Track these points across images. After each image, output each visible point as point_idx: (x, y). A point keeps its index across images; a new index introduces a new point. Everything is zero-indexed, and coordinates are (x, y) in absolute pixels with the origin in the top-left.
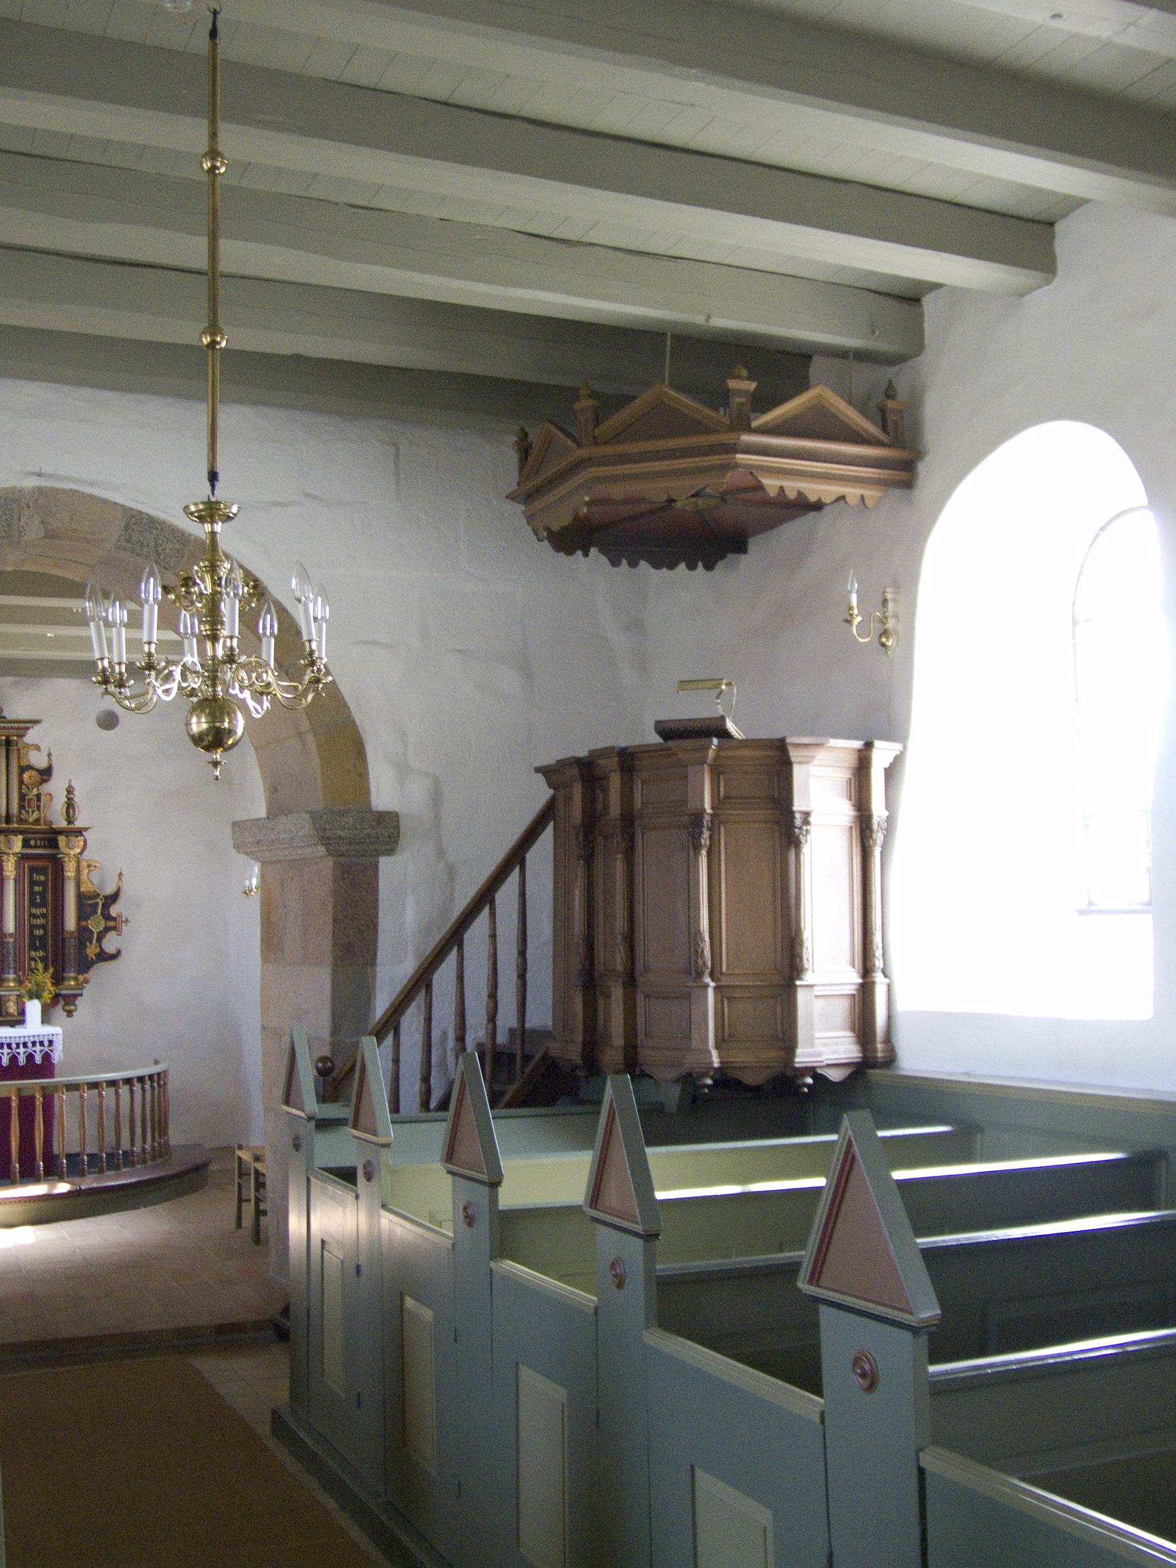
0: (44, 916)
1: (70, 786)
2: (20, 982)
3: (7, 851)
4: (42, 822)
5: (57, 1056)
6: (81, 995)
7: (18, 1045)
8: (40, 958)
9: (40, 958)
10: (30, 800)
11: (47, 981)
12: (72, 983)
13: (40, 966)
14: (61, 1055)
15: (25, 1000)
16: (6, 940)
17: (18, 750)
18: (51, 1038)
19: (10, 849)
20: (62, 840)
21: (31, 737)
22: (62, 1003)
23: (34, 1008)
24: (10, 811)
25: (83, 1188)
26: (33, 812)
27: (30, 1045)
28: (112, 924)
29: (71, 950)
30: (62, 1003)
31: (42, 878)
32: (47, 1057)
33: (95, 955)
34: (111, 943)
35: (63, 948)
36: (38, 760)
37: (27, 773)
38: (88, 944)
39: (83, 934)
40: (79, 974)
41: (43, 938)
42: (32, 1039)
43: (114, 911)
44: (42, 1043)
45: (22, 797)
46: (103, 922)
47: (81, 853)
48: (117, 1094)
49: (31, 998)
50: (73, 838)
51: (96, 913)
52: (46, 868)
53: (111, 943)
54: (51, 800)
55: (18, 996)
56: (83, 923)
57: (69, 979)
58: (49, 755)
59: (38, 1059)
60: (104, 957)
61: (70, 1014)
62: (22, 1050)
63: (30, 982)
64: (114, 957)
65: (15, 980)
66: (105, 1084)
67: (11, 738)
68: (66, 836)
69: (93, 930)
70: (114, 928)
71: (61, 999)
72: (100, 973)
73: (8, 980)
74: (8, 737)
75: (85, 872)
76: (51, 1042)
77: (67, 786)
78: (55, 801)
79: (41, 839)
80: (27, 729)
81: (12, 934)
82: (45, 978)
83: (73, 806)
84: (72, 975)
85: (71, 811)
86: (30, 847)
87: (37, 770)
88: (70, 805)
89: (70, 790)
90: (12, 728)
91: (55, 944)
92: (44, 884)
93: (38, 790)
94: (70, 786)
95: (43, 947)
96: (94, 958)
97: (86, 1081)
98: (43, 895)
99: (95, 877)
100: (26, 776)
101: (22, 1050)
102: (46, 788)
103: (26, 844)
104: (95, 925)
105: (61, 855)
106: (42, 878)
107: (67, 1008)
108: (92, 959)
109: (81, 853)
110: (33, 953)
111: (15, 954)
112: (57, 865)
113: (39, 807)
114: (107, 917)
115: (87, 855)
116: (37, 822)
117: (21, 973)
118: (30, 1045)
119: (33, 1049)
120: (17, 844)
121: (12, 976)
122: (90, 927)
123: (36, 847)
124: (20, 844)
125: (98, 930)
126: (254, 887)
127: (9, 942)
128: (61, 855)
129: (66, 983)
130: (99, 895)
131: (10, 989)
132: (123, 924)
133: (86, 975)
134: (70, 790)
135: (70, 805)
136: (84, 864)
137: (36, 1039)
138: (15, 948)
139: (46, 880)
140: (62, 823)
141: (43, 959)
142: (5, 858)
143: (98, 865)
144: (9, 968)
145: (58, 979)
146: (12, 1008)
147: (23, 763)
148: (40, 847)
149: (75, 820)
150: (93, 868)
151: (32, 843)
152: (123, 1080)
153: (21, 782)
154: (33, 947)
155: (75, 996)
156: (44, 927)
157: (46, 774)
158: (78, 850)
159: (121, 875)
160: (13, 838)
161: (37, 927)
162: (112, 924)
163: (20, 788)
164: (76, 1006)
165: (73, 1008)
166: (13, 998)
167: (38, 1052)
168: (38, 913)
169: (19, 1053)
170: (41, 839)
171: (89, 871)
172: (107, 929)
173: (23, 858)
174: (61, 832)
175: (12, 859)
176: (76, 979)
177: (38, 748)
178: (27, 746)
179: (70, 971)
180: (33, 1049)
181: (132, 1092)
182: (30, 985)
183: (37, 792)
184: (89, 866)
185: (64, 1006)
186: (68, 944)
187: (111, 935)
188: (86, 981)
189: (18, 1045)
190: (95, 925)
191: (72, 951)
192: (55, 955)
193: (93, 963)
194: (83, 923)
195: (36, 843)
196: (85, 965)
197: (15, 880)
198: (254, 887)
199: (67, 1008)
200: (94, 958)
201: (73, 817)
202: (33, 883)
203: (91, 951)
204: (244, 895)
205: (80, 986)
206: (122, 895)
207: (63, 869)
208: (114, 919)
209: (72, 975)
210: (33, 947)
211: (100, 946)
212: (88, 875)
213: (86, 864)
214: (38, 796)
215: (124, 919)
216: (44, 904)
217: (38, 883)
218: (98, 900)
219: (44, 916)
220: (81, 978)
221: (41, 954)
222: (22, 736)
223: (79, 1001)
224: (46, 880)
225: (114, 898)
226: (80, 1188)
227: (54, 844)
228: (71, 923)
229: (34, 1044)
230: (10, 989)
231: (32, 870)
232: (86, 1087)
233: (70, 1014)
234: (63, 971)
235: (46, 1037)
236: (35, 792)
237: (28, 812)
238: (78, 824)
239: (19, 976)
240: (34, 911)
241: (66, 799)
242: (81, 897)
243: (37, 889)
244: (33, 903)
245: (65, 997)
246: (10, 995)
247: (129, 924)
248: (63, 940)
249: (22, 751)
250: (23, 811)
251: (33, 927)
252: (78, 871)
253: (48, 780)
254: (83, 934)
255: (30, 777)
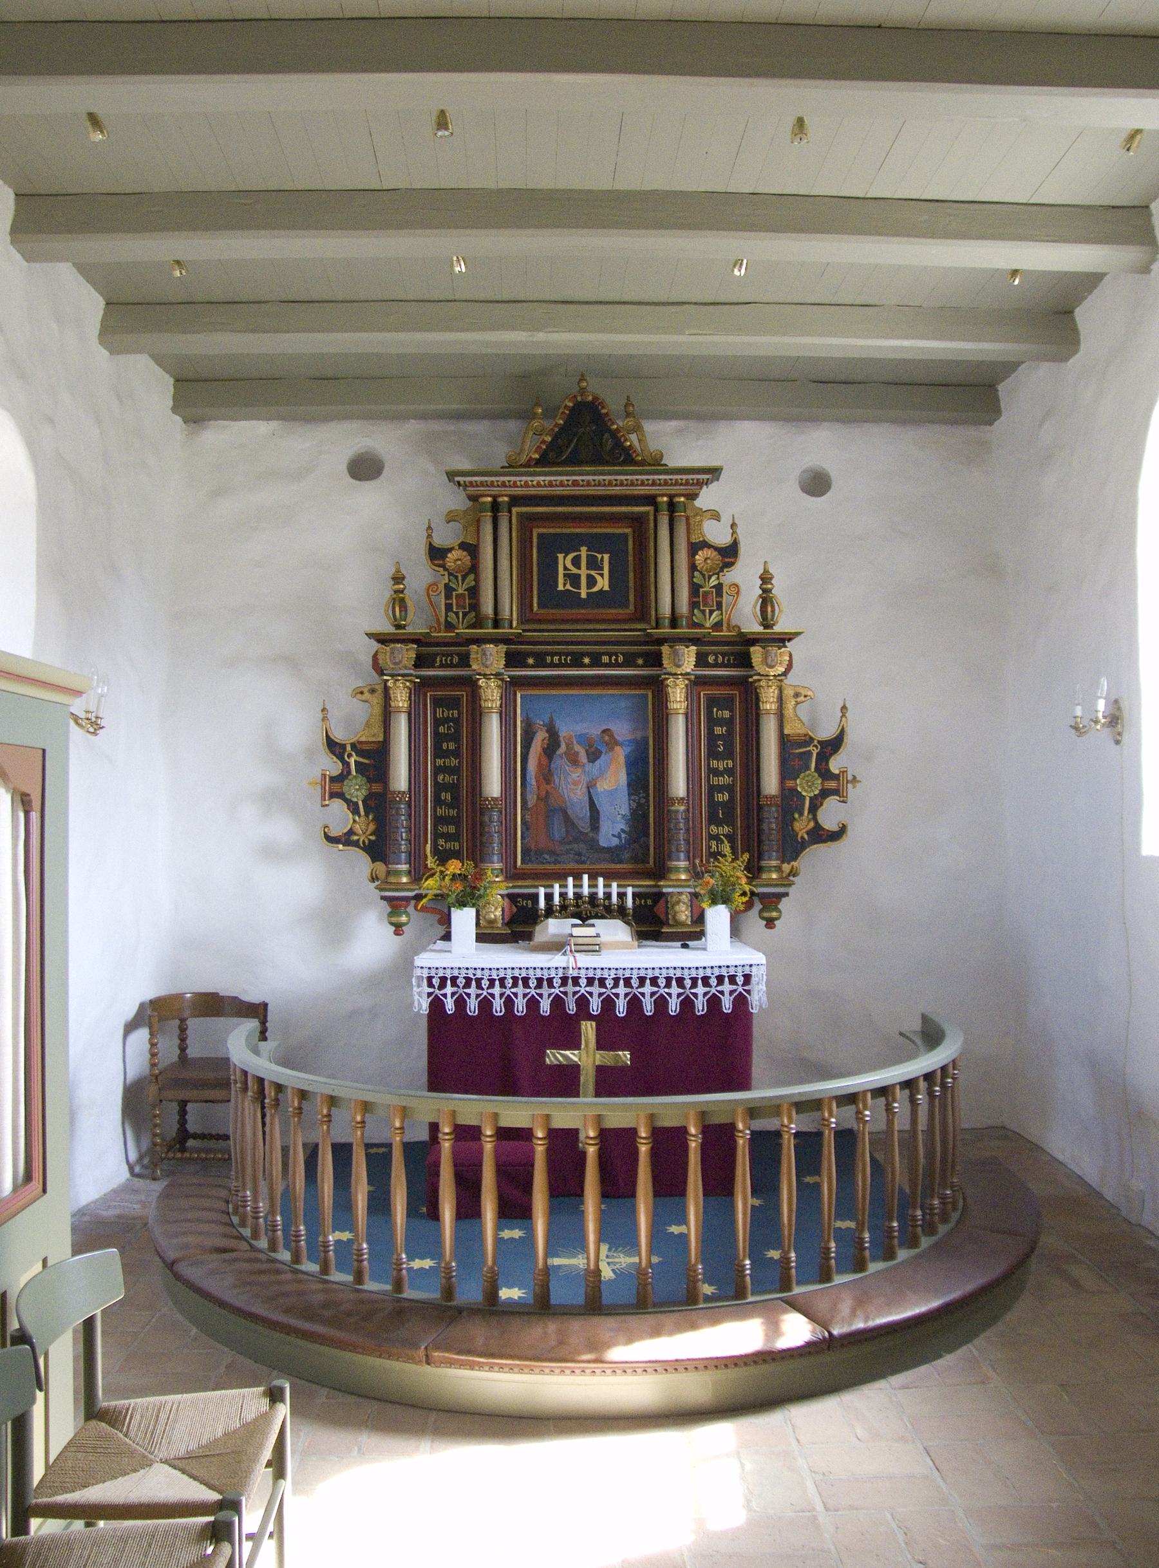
0: (730, 772)
1: (766, 571)
2: (697, 875)
3: (674, 670)
4: (725, 625)
5: (758, 997)
6: (786, 894)
7: (694, 981)
8: (726, 836)
9: (726, 836)
10: (706, 594)
11: (739, 874)
12: (774, 876)
13: (726, 848)
14: (764, 999)
15: (704, 905)
16: (673, 808)
17: (688, 518)
18: (747, 970)
19: (679, 666)
20: (756, 652)
21: (706, 499)
22: (758, 906)
23: (718, 918)
24: (677, 610)
25: (835, 1332)
26: (711, 612)
27: (713, 981)
28: (832, 785)
29: (771, 824)
30: (758, 906)
31: (726, 714)
32: (741, 1001)
33: (807, 833)
34: (830, 815)
35: (760, 821)
36: (717, 534)
37: (700, 553)
38: (796, 816)
39: (789, 800)
40: (783, 862)
41: (729, 806)
42: (717, 972)
43: (835, 765)
44: (733, 980)
45: (695, 589)
46: (820, 781)
47: (785, 674)
48: (889, 1109)
49: (714, 902)
50: (773, 650)
51: (808, 768)
52: (731, 699)
53: (830, 815)
54: (738, 593)
55: (695, 895)
56: (790, 784)
57: (770, 869)
58: (733, 525)
59: (727, 1005)
60: (820, 836)
61: (770, 923)
62: (700, 990)
63: (712, 877)
64: (837, 835)
65: (687, 870)
66: (869, 1095)
67: (677, 499)
68: (764, 648)
69: (804, 793)
70: (836, 792)
71: (756, 899)
72: (815, 858)
73: (677, 870)
74: (671, 497)
75: (790, 704)
76: (747, 978)
77: (762, 571)
78: (742, 600)
79: (724, 655)
80: (700, 484)
81: (682, 799)
82: (733, 869)
83: (772, 603)
84: (774, 863)
85: (769, 609)
86: (707, 665)
87: (716, 549)
88: (766, 599)
89: (766, 578)
90: (676, 483)
91: (747, 815)
92: (730, 723)
93: (718, 578)
94: (766, 571)
95: (729, 820)
96: (806, 836)
97: (834, 1094)
98: (728, 738)
99: (803, 712)
100: (699, 557)
101: (700, 990)
102: (730, 577)
103: (701, 661)
104: (807, 786)
105: (755, 678)
106: (726, 714)
107: (766, 915)
108: (802, 838)
109: (785, 674)
110: (714, 829)
111: (688, 830)
112: (749, 693)
113: (719, 606)
114: (825, 773)
115: (790, 680)
116: (718, 626)
117: (697, 861)
118: (713, 981)
119: (719, 988)
120: (688, 658)
121: (683, 864)
122: (799, 790)
123: (716, 665)
124: (693, 659)
125: (812, 794)
126: (1100, 715)
127: (677, 811)
128: (755, 678)
129: (764, 876)
130: (812, 739)
131: (681, 884)
132: (850, 786)
133: (795, 864)
134: (766, 578)
135: (766, 599)
136: (789, 692)
137: (724, 972)
138: (687, 820)
139: (732, 718)
140: (753, 626)
141: (731, 838)
142: (670, 681)
143: (810, 693)
144: (678, 851)
145: (754, 870)
146: (683, 913)
147: (695, 539)
148: (723, 665)
149: (774, 625)
150: (801, 699)
151: (711, 659)
152: (900, 1083)
153: (693, 567)
154: (713, 819)
155: (780, 896)
156: (730, 789)
157: (729, 554)
158: (781, 669)
159: (844, 708)
160: (681, 648)
161: (721, 789)
162: (832, 785)
163: (691, 577)
164: (779, 911)
165: (774, 914)
166: (684, 898)
167: (727, 994)
168: (721, 768)
169: (695, 995)
170: (724, 655)
171: (797, 703)
172: (825, 793)
173: (697, 683)
174: (751, 641)
175: (682, 683)
176: (779, 869)
177: (716, 516)
178: (700, 512)
179: (770, 859)
180: (719, 988)
181: (913, 1101)
182: (712, 881)
183: (716, 582)
184: (797, 695)
185: (761, 911)
186: (766, 815)
187: (831, 802)
188: (794, 873)
189: (694, 981)
190: (807, 786)
191: (774, 826)
192: (747, 827)
193: (803, 845)
194: (790, 784)
195: (716, 660)
196: (792, 848)
197: (686, 714)
198: (1100, 715)
199: (766, 915)
200: (806, 836)
201: (772, 620)
202: (712, 722)
203: (802, 826)
204: (1073, 731)
205: (787, 880)
206: (849, 739)
207: (758, 699)
208: (836, 777)
209: (774, 863)
210: (713, 819)
211: (815, 819)
212: (795, 708)
213: (792, 693)
214: (719, 588)
215: (850, 778)
216: (729, 754)
217: (720, 722)
218: (811, 748)
219: (730, 772)
220: (786, 867)
221: (726, 829)
222: (693, 497)
223: (784, 904)
224: (732, 718)
225: (835, 744)
226: (830, 1334)
227: (744, 661)
228: (771, 783)
229: (720, 979)
230: (681, 884)
231: (712, 702)
232: (834, 1105)
233: (770, 923)
234: (760, 858)
235: (740, 969)
236: (713, 581)
237: (703, 612)
238: (781, 626)
239: (694, 865)
240: (714, 763)
241: (761, 592)
242: (784, 741)
243: (718, 730)
244: (712, 754)
245: (763, 897)
246: (680, 894)
247: (858, 785)
248: (760, 808)
249: (692, 522)
250: (695, 611)
251: (712, 789)
252: (780, 700)
253: (732, 564)
254: (789, 800)
255: (706, 559)
